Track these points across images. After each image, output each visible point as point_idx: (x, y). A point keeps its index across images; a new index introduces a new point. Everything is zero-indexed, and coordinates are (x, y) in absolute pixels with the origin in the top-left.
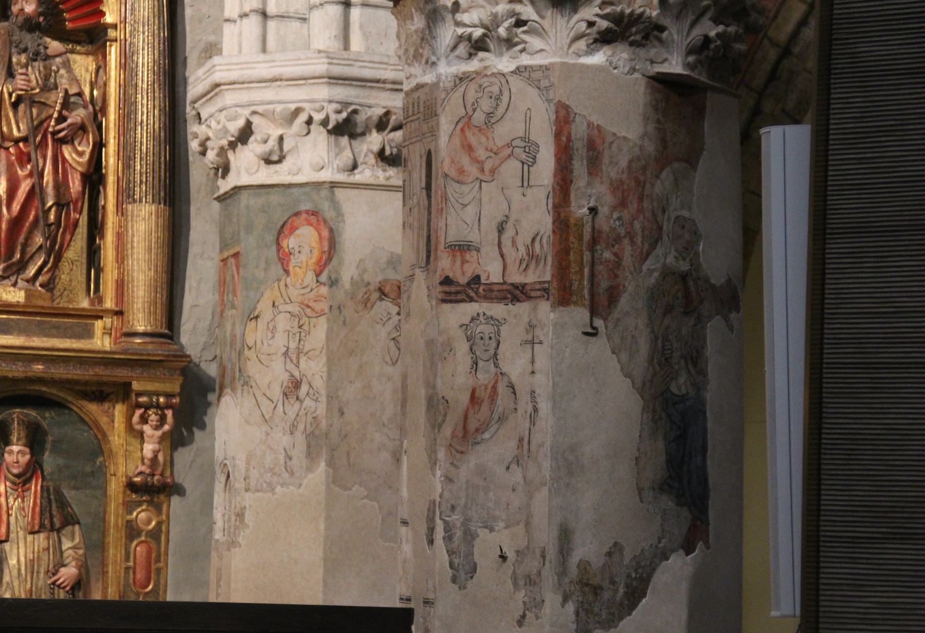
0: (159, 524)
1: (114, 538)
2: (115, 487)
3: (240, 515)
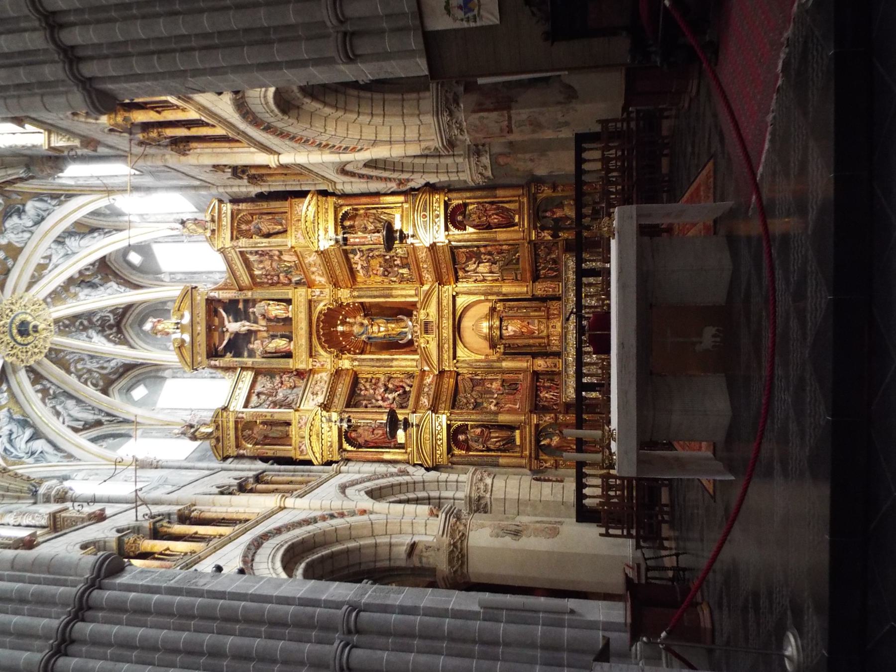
1: (564, 194)
2: (554, 195)
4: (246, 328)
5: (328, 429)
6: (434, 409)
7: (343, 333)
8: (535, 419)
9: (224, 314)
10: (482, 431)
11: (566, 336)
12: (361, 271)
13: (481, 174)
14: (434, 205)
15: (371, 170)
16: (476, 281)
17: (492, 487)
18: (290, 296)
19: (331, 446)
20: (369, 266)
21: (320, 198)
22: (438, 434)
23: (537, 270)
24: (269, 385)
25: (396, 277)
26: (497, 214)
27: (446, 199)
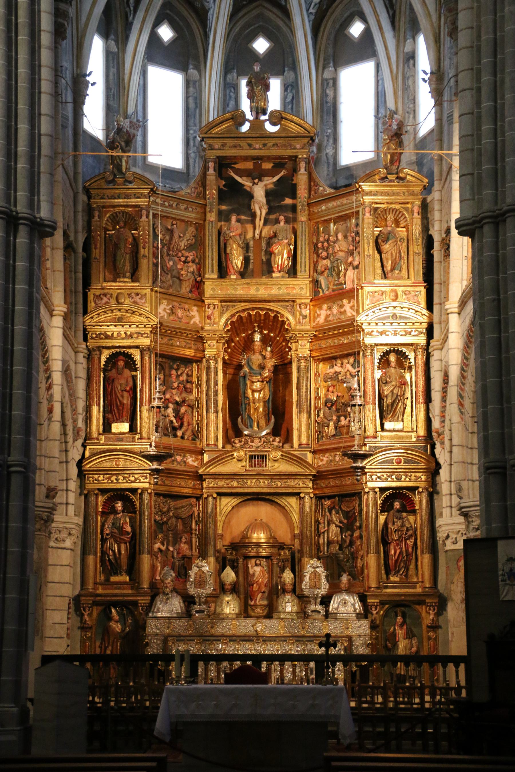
4: (258, 212)
5: (129, 333)
10: (128, 533)
12: (332, 370)
14: (413, 474)
16: (318, 522)
18: (299, 275)
19: (107, 337)
20: (338, 381)
21: (425, 326)
24: (183, 244)
25: (324, 417)
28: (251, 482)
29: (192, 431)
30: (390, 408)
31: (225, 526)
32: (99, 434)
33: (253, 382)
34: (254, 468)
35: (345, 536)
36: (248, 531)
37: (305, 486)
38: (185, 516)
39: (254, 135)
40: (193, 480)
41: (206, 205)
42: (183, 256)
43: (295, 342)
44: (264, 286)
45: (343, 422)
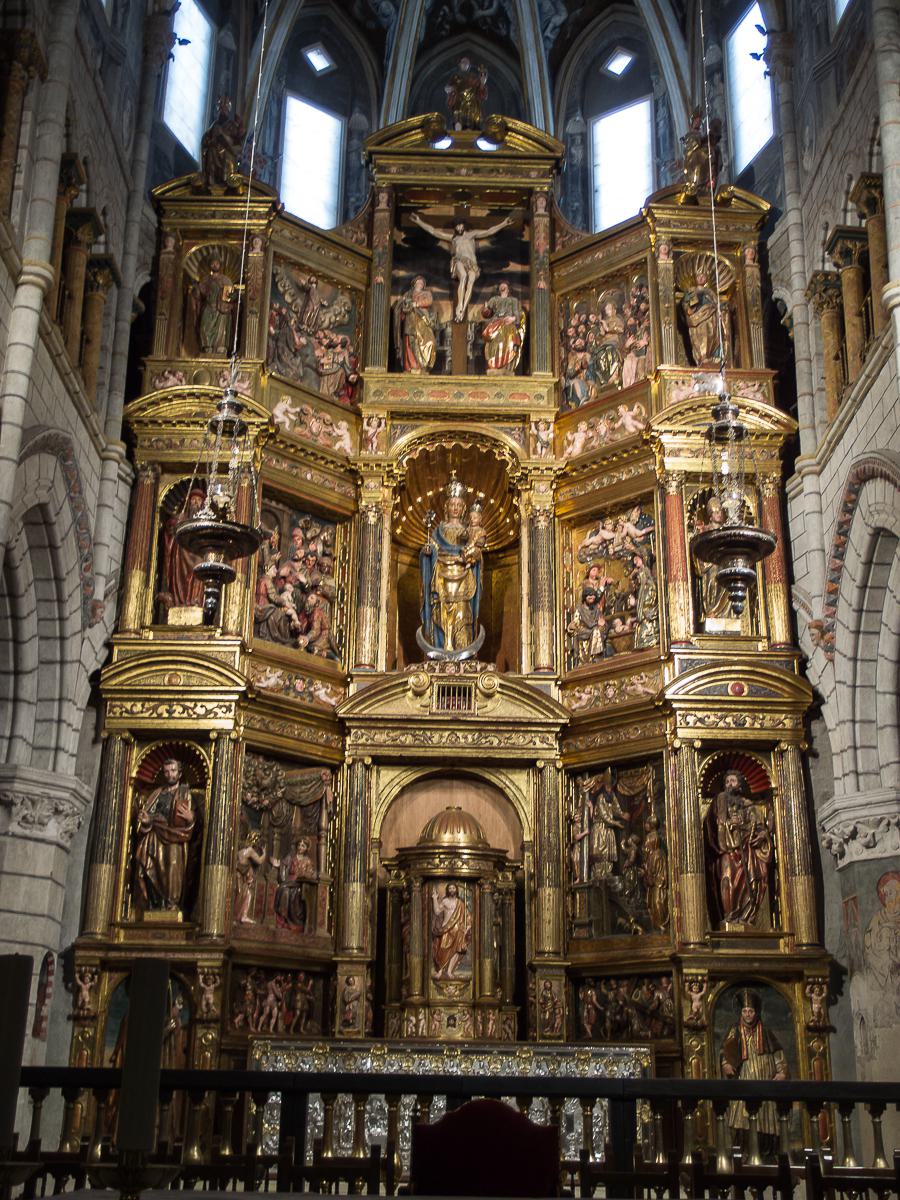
0: (824, 1049)
2: (799, 1028)
3: (874, 1041)
4: (463, 274)
6: (251, 699)
7: (444, 497)
8: (208, 961)
9: (493, 230)
10: (186, 823)
11: (430, 1052)
12: (596, 539)
13: (854, 835)
14: (768, 716)
15: (863, 551)
16: (570, 820)
17: (37, 840)
19: (170, 446)
20: (608, 557)
22: (185, 708)
23: (597, 979)
24: (327, 318)
25: (581, 621)
26: (745, 874)
27: (784, 746)
28: (441, 737)
29: (329, 641)
30: (715, 592)
31: (387, 827)
32: (143, 627)
33: (446, 565)
34: (446, 711)
35: (626, 845)
36: (432, 829)
37: (545, 746)
38: (307, 802)
39: (459, 151)
40: (326, 729)
41: (370, 260)
42: (325, 337)
43: (526, 490)
44: (471, 389)
45: (619, 627)
